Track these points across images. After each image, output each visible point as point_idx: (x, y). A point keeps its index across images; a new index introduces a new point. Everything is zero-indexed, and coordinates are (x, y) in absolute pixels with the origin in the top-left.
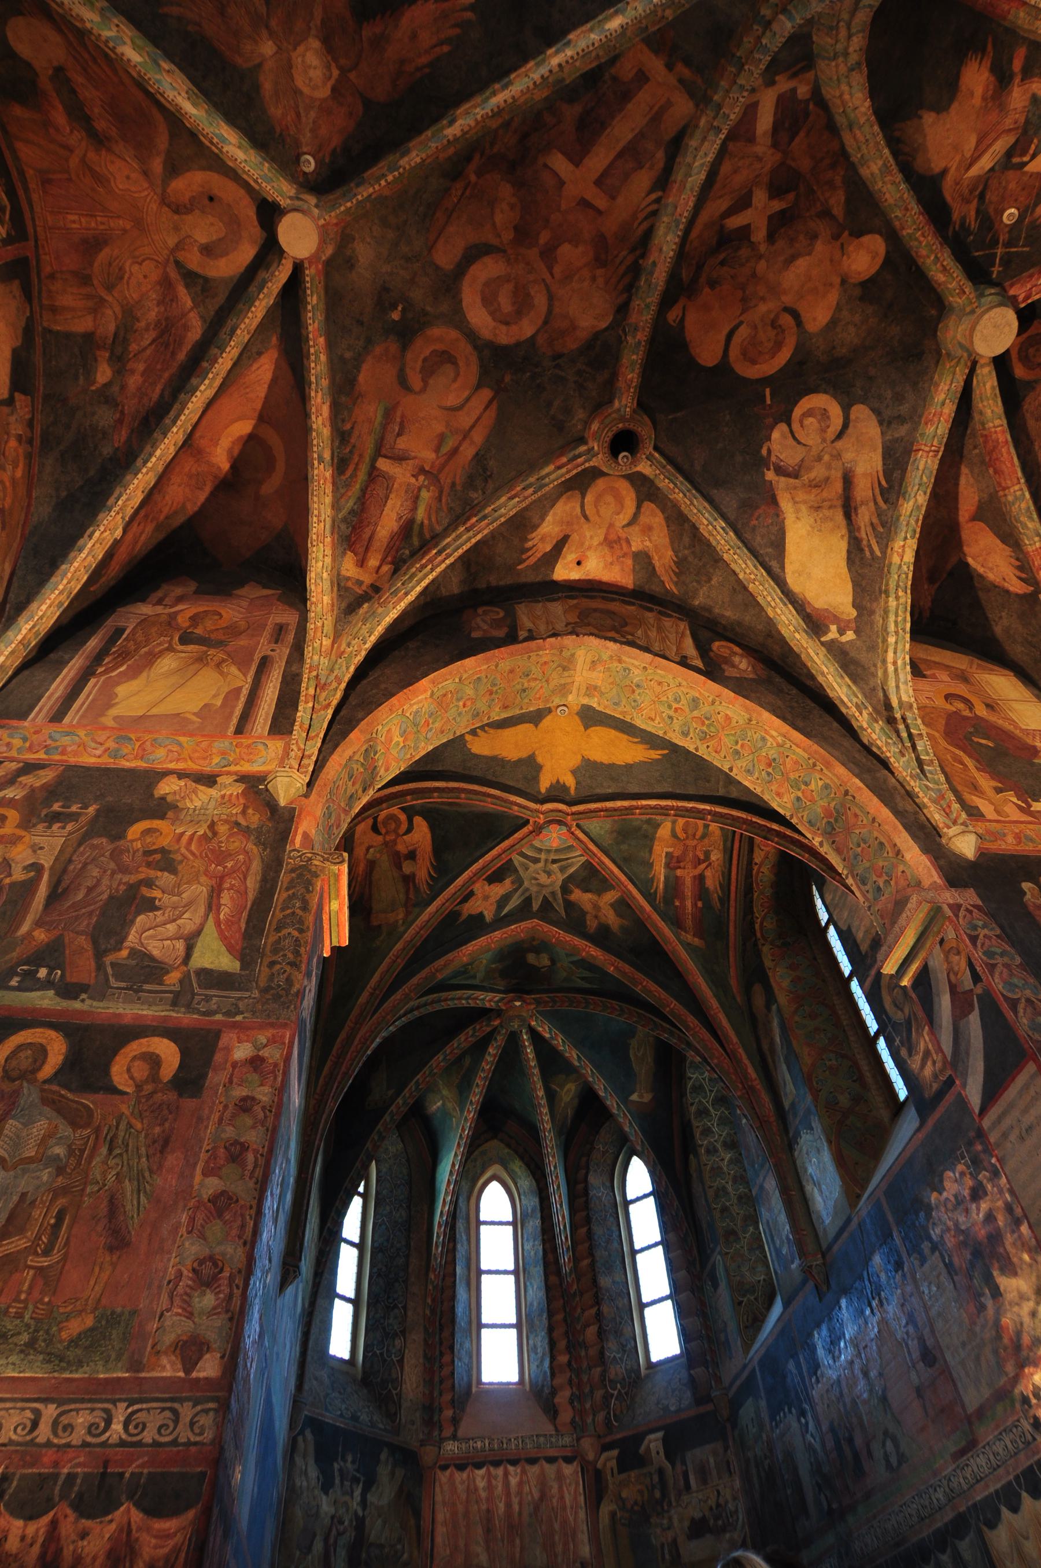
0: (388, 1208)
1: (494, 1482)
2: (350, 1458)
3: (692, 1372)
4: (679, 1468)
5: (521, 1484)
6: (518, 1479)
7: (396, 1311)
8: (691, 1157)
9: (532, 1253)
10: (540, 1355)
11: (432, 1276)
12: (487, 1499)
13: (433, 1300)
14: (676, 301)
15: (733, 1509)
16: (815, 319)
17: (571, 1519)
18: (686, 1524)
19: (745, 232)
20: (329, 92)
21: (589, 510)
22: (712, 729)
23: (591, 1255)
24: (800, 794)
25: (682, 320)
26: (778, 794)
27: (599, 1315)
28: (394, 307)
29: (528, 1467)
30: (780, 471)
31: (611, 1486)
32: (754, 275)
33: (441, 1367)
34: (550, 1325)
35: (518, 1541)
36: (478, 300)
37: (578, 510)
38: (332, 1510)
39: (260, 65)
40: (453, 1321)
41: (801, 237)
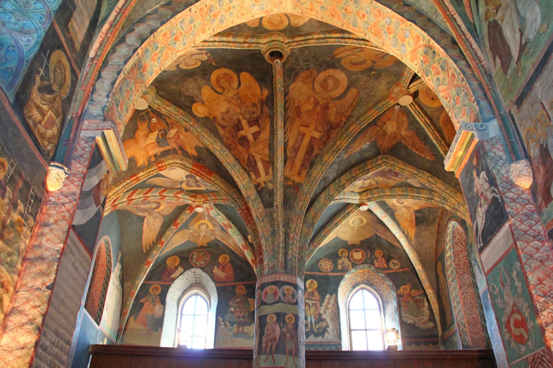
14: (266, 98)
16: (208, 90)
19: (250, 126)
20: (387, 123)
21: (286, 20)
22: (208, 18)
24: (158, 51)
25: (261, 91)
26: (165, 34)
28: (374, 75)
30: (201, 53)
32: (240, 107)
36: (341, 82)
37: (291, 19)
39: (406, 130)
41: (228, 120)
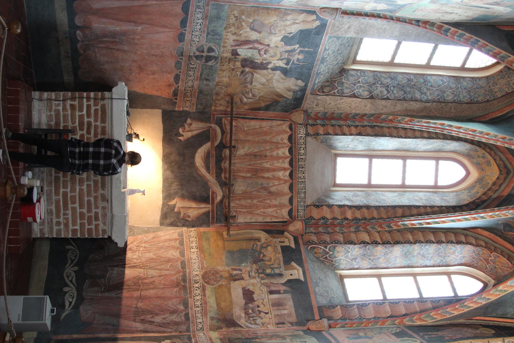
0: (454, 86)
1: (281, 161)
2: (301, 57)
3: (339, 307)
4: (282, 288)
5: (279, 179)
6: (282, 177)
7: (386, 92)
8: (493, 332)
9: (417, 198)
10: (351, 198)
11: (407, 119)
12: (272, 156)
13: (391, 120)
15: (257, 322)
17: (258, 212)
18: (251, 288)
23: (415, 243)
27: (375, 243)
29: (288, 184)
31: (274, 240)
33: (349, 126)
34: (371, 207)
35: (249, 175)
38: (272, 45)
40: (376, 135)
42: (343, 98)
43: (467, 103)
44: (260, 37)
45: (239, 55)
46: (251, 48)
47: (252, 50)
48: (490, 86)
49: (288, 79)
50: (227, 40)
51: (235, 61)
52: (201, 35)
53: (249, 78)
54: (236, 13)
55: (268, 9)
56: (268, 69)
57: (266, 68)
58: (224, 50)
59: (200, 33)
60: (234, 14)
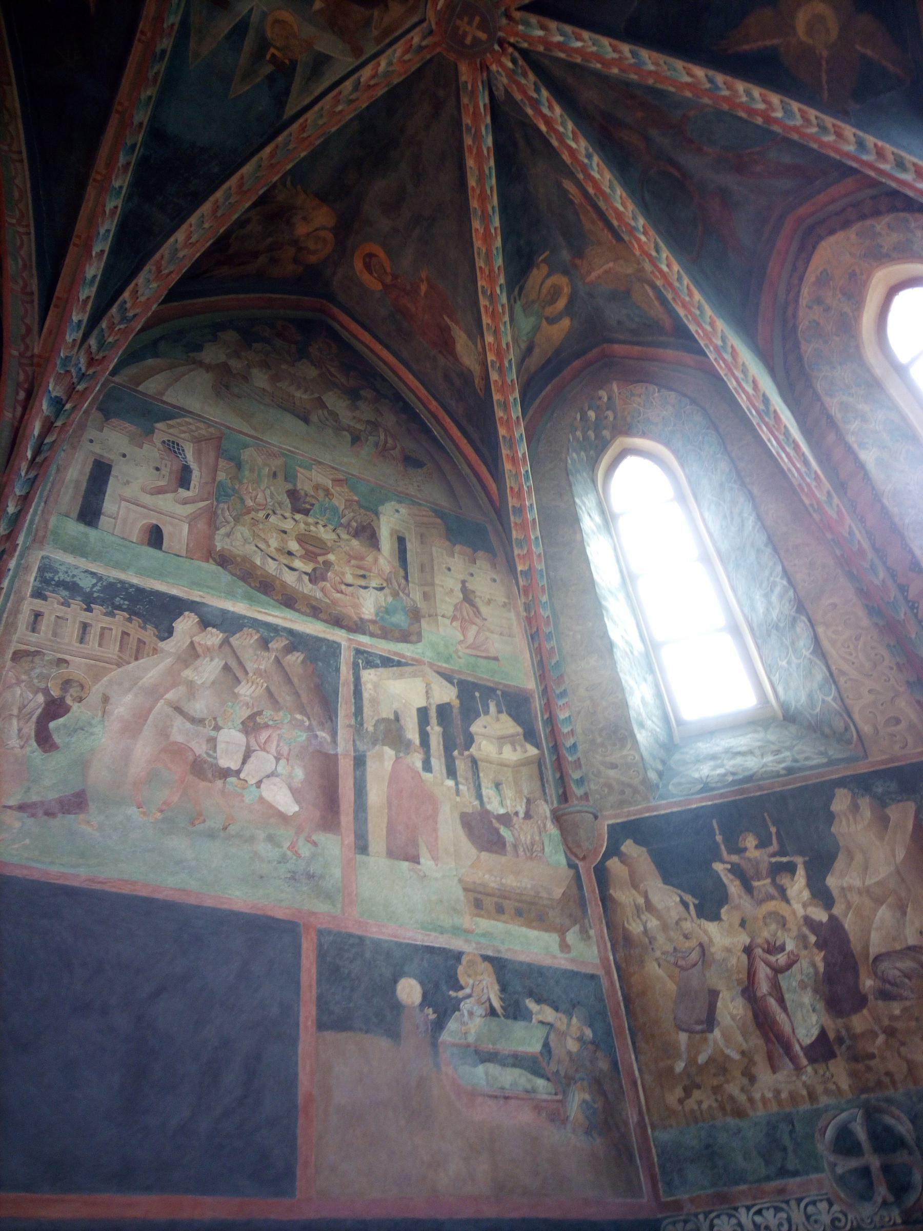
42: (835, 672)
43: (716, 429)
44: (729, 989)
45: (823, 1034)
46: (781, 1001)
47: (787, 996)
48: (675, 425)
49: (841, 844)
50: (784, 1095)
51: (854, 1037)
52: (799, 1201)
53: (898, 964)
54: (673, 1097)
55: (628, 1000)
56: (832, 918)
57: (835, 924)
58: (827, 1092)
59: (793, 1204)
60: (681, 1101)
